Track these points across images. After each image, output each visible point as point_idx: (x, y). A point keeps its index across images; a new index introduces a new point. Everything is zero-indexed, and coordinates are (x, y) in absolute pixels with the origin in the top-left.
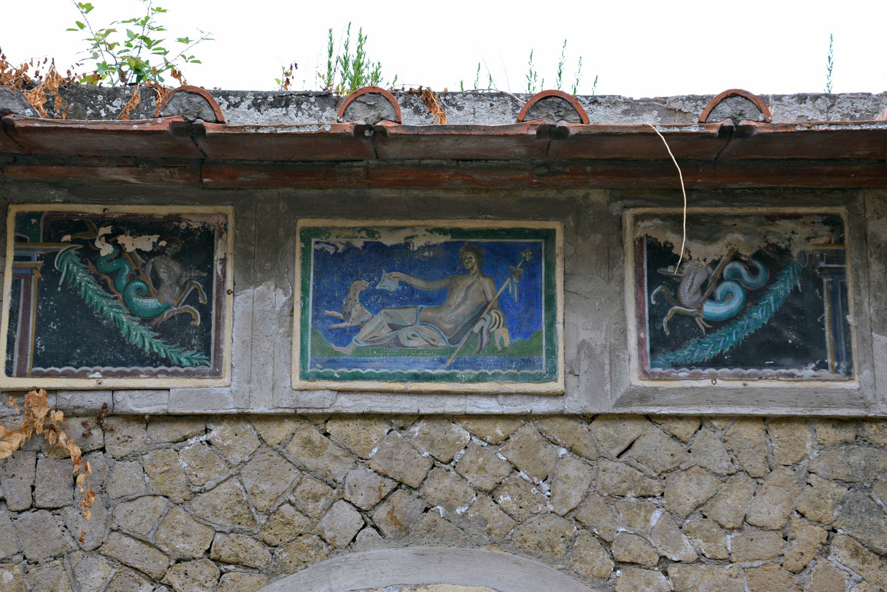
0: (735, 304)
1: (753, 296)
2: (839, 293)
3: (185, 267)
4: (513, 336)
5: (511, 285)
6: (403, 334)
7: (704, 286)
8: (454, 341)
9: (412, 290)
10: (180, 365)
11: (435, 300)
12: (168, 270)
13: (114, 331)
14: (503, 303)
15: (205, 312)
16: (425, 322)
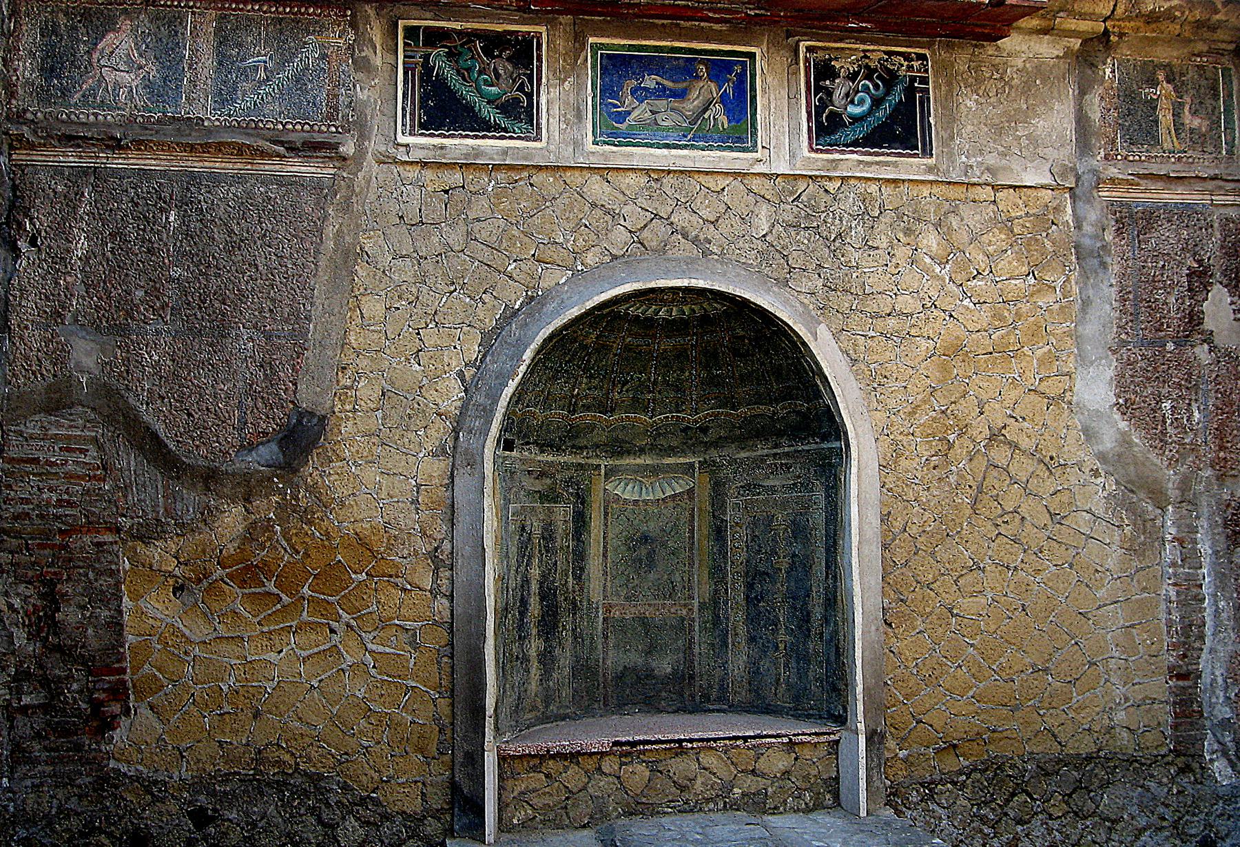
0: (866, 107)
1: (877, 102)
2: (925, 101)
3: (515, 66)
4: (729, 121)
5: (728, 88)
6: (659, 117)
7: (847, 95)
8: (693, 123)
9: (664, 88)
10: (514, 132)
11: (681, 95)
12: (504, 67)
13: (470, 109)
14: (723, 99)
15: (529, 96)
16: (672, 110)
